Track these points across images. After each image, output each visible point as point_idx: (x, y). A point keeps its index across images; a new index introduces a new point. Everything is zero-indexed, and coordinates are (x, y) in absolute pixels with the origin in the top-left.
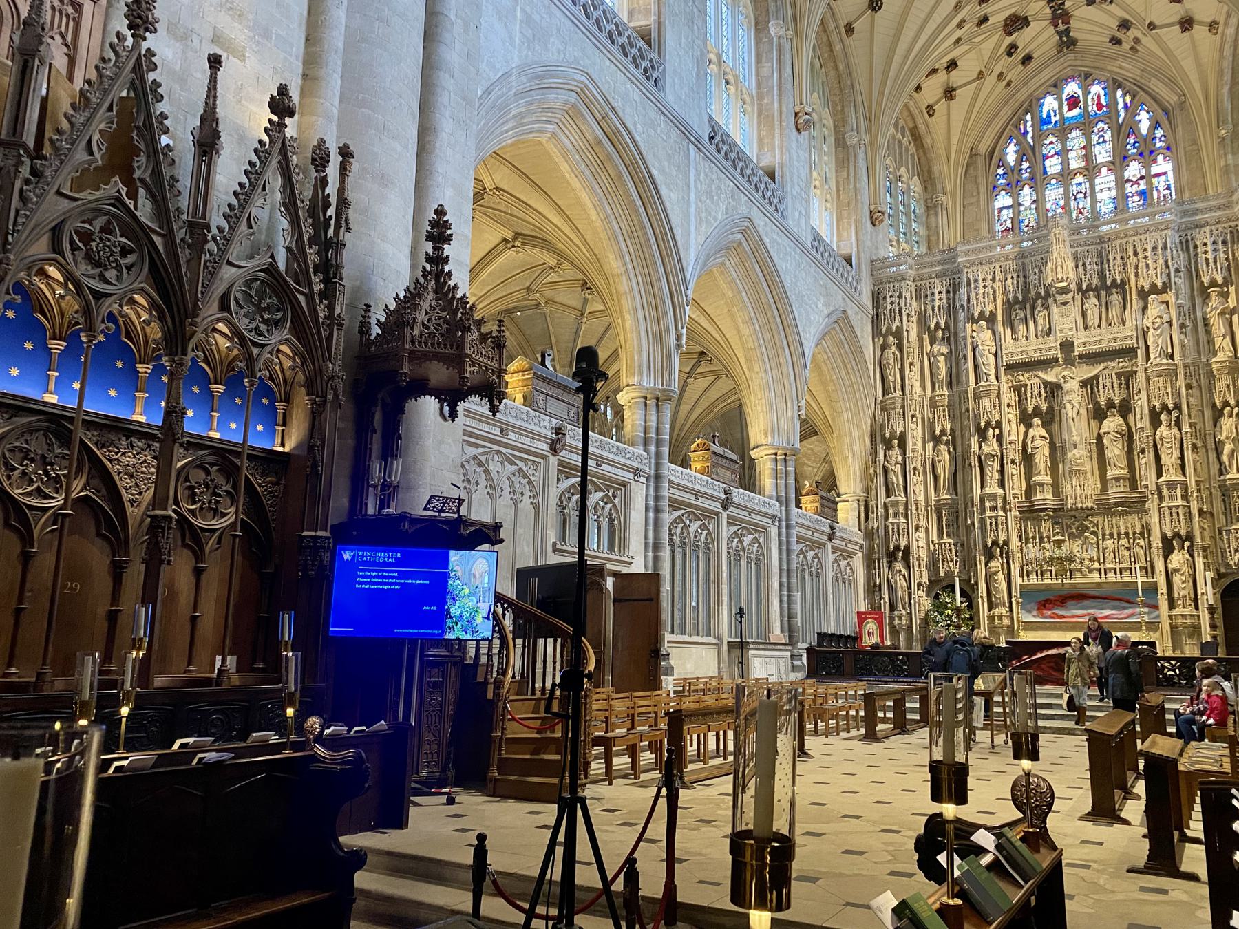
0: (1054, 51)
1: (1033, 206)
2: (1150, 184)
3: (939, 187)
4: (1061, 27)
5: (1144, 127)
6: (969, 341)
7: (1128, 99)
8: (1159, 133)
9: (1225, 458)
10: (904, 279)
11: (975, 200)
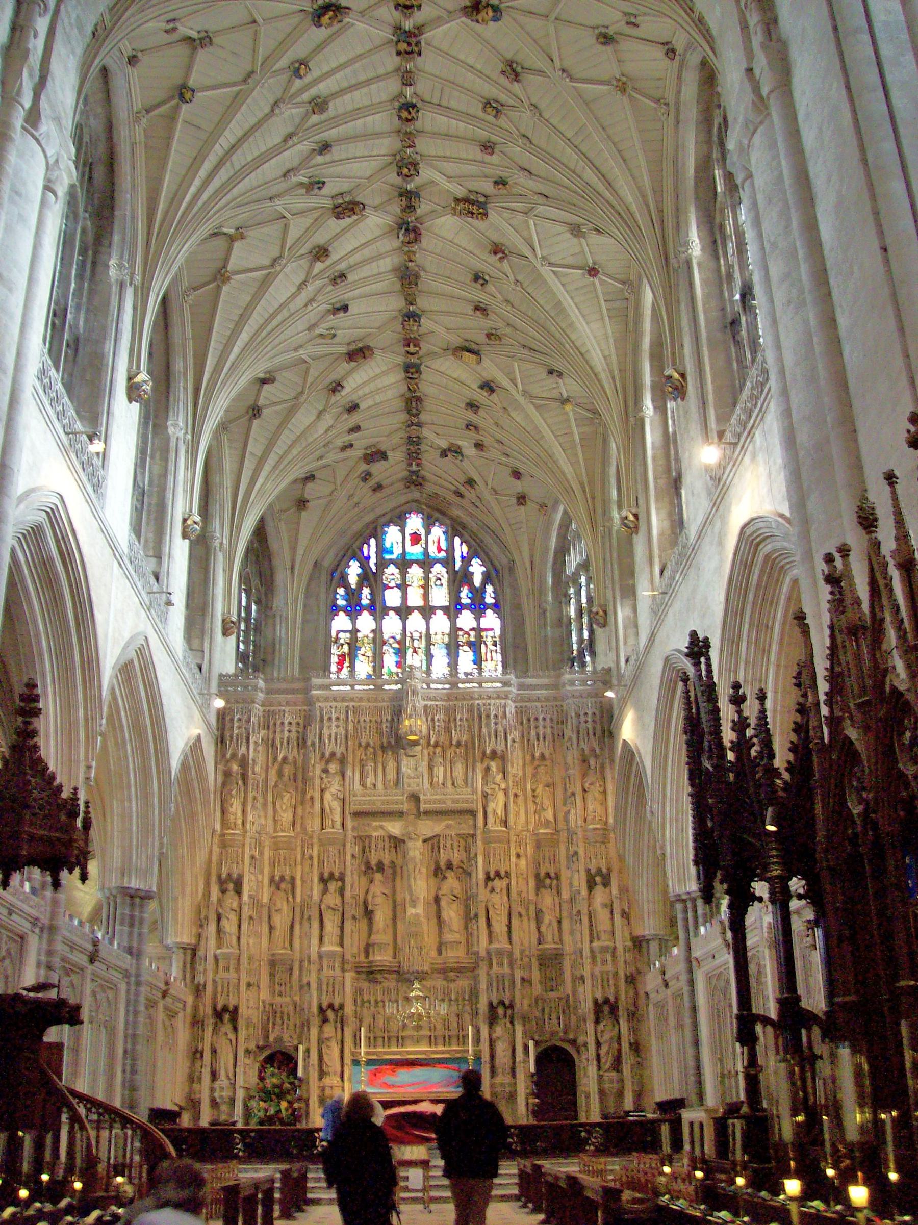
1: (371, 635)
4: (414, 468)
5: (477, 581)
6: (317, 781)
7: (465, 549)
8: (489, 589)
9: (543, 929)
10: (253, 702)
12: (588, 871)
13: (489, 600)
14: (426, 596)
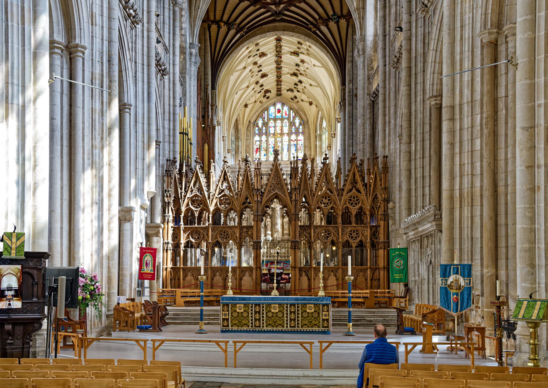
0: (275, 95)
2: (297, 142)
4: (279, 93)
5: (297, 124)
7: (294, 114)
8: (301, 127)
11: (249, 138)
12: (321, 217)
13: (301, 131)
14: (282, 130)
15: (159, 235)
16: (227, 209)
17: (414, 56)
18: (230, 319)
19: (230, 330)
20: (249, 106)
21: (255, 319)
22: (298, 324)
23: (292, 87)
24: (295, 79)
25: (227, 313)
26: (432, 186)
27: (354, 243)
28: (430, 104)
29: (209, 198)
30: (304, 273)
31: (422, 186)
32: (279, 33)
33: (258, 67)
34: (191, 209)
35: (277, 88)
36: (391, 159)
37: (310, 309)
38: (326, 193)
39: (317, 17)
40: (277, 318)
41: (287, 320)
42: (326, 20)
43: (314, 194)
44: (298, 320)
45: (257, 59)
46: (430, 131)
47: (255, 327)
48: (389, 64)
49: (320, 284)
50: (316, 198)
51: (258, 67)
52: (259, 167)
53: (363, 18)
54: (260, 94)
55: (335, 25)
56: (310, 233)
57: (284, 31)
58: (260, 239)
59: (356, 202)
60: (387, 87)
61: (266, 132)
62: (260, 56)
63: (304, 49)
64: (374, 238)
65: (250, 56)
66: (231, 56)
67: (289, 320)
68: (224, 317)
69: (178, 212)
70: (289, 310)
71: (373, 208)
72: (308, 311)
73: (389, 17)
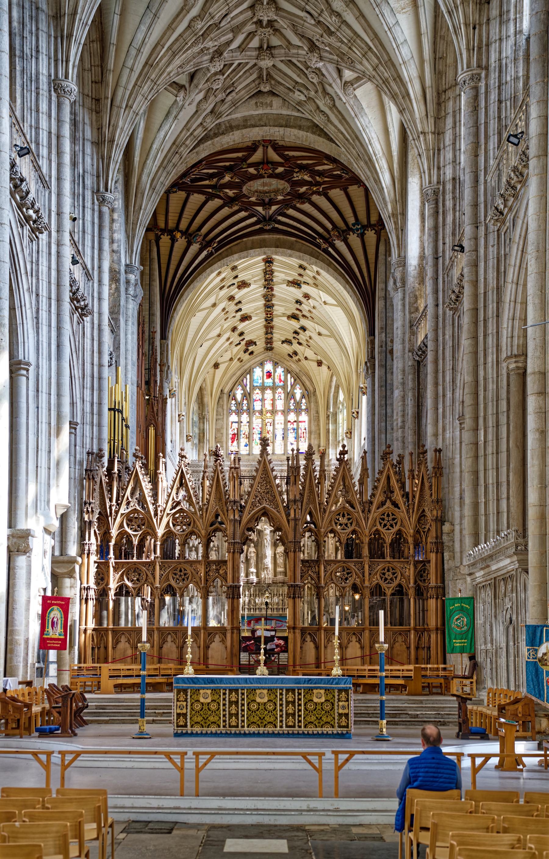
0: (263, 350)
2: (298, 425)
3: (206, 409)
4: (269, 345)
5: (298, 396)
7: (293, 380)
8: (304, 401)
11: (221, 417)
13: (304, 407)
14: (273, 405)
15: (74, 575)
16: (185, 533)
17: (483, 292)
18: (189, 714)
19: (189, 732)
20: (221, 366)
21: (229, 713)
22: (300, 721)
23: (290, 336)
24: (295, 325)
25: (185, 703)
26: (511, 499)
27: (388, 588)
28: (508, 368)
29: (156, 514)
30: (308, 636)
31: (495, 498)
32: (269, 251)
33: (236, 304)
34: (126, 532)
35: (267, 338)
36: (447, 454)
37: (319, 697)
38: (344, 507)
39: (329, 226)
40: (266, 713)
41: (281, 716)
42: (343, 231)
43: (324, 509)
44: (300, 716)
45: (234, 291)
46: (508, 410)
47: (230, 726)
48: (444, 303)
49: (334, 655)
50: (328, 516)
51: (236, 304)
52: (237, 466)
53: (402, 230)
54: (239, 347)
55: (358, 240)
56: (319, 572)
57: (277, 247)
58: (238, 581)
59: (391, 522)
60: (441, 339)
61: (249, 409)
62: (239, 287)
63: (309, 276)
64: (421, 581)
65: (223, 287)
66: (192, 286)
67: (284, 716)
68: (179, 711)
69: (105, 536)
70: (284, 699)
71: (418, 532)
72: (316, 700)
73: (444, 230)
